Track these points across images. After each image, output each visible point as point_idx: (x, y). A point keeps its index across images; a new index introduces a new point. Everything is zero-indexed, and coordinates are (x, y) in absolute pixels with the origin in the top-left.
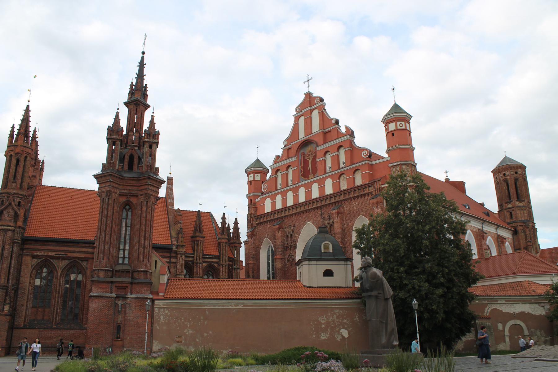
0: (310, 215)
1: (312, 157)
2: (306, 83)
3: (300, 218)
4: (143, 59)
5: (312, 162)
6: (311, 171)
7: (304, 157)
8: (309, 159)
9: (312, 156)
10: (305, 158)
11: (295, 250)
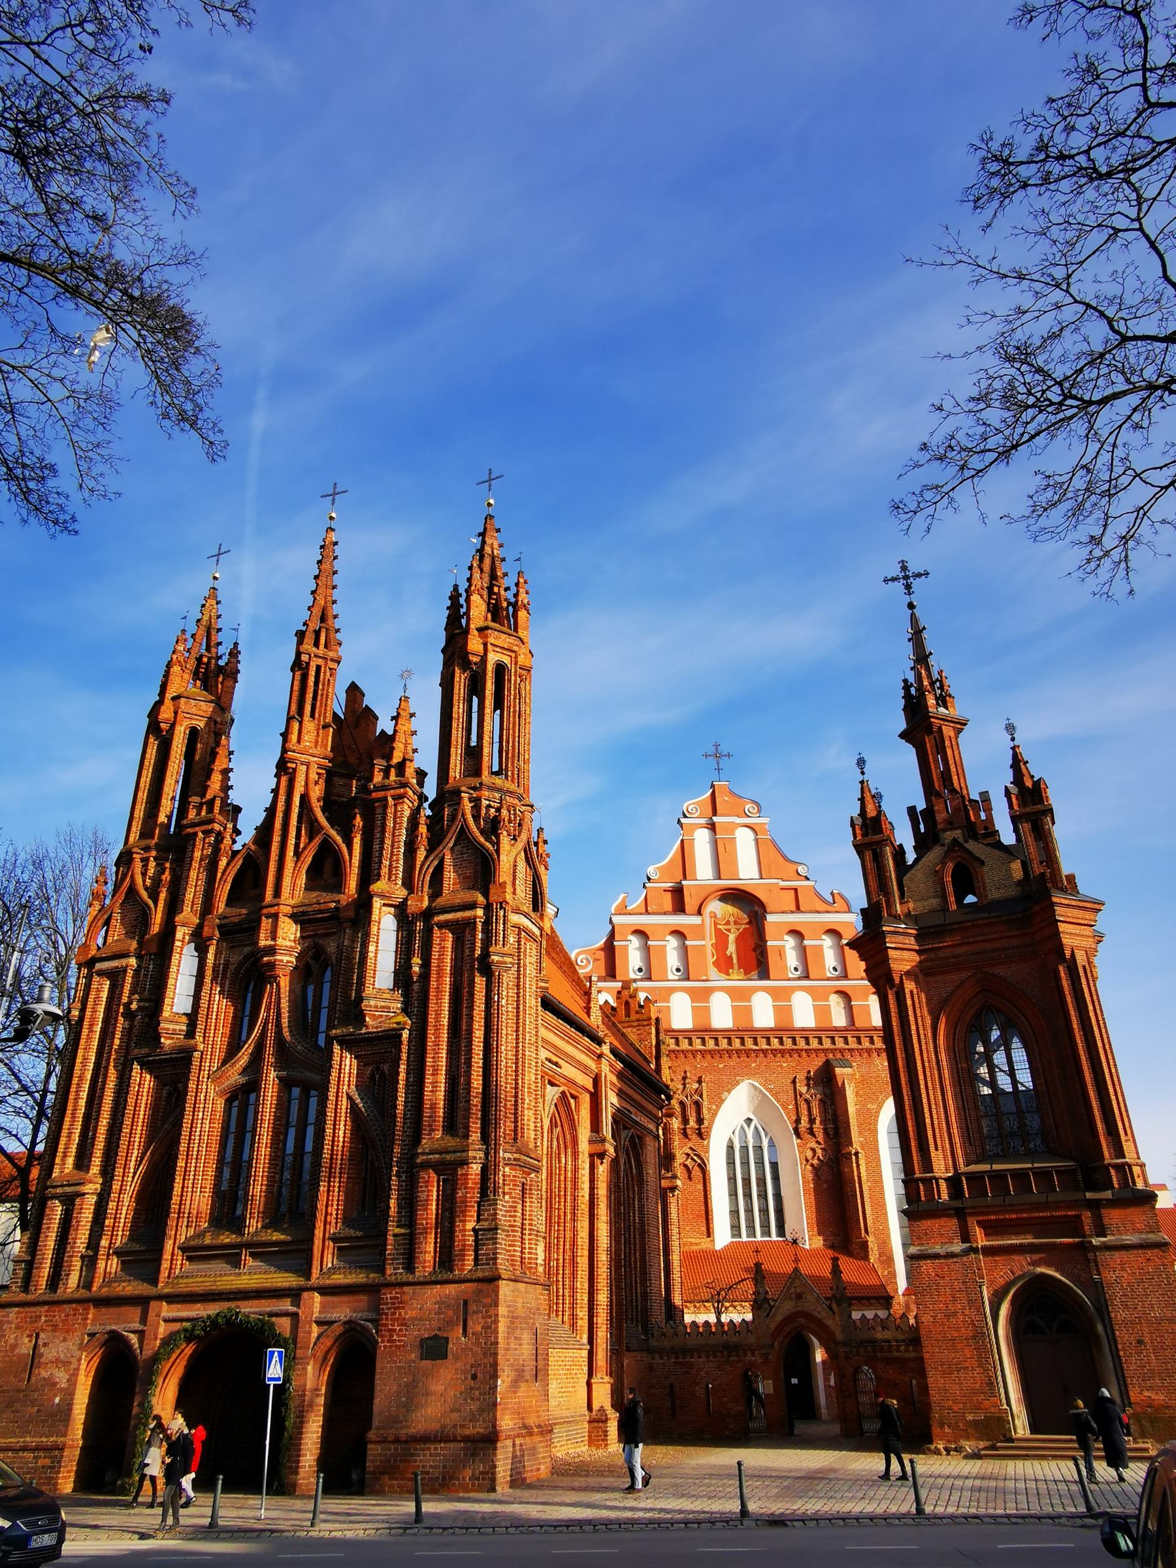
0: (753, 1065)
1: (738, 930)
2: (712, 761)
3: (721, 1066)
4: (914, 620)
5: (738, 940)
6: (735, 961)
7: (716, 924)
8: (729, 930)
9: (738, 927)
10: (719, 926)
11: (705, 1143)
